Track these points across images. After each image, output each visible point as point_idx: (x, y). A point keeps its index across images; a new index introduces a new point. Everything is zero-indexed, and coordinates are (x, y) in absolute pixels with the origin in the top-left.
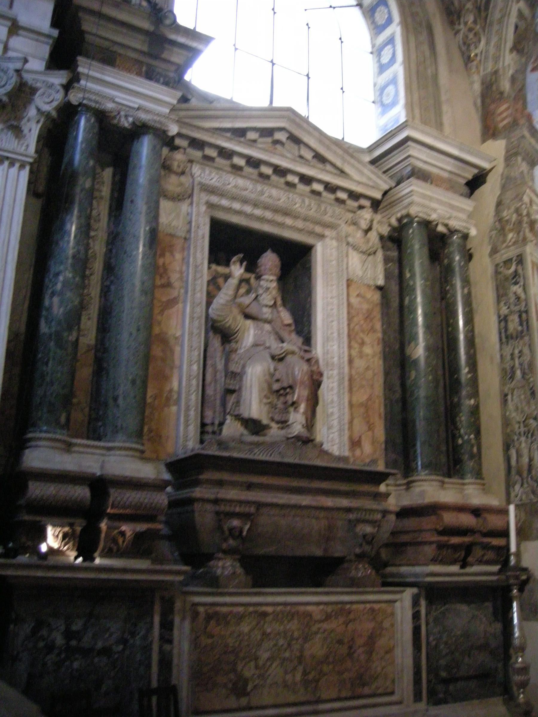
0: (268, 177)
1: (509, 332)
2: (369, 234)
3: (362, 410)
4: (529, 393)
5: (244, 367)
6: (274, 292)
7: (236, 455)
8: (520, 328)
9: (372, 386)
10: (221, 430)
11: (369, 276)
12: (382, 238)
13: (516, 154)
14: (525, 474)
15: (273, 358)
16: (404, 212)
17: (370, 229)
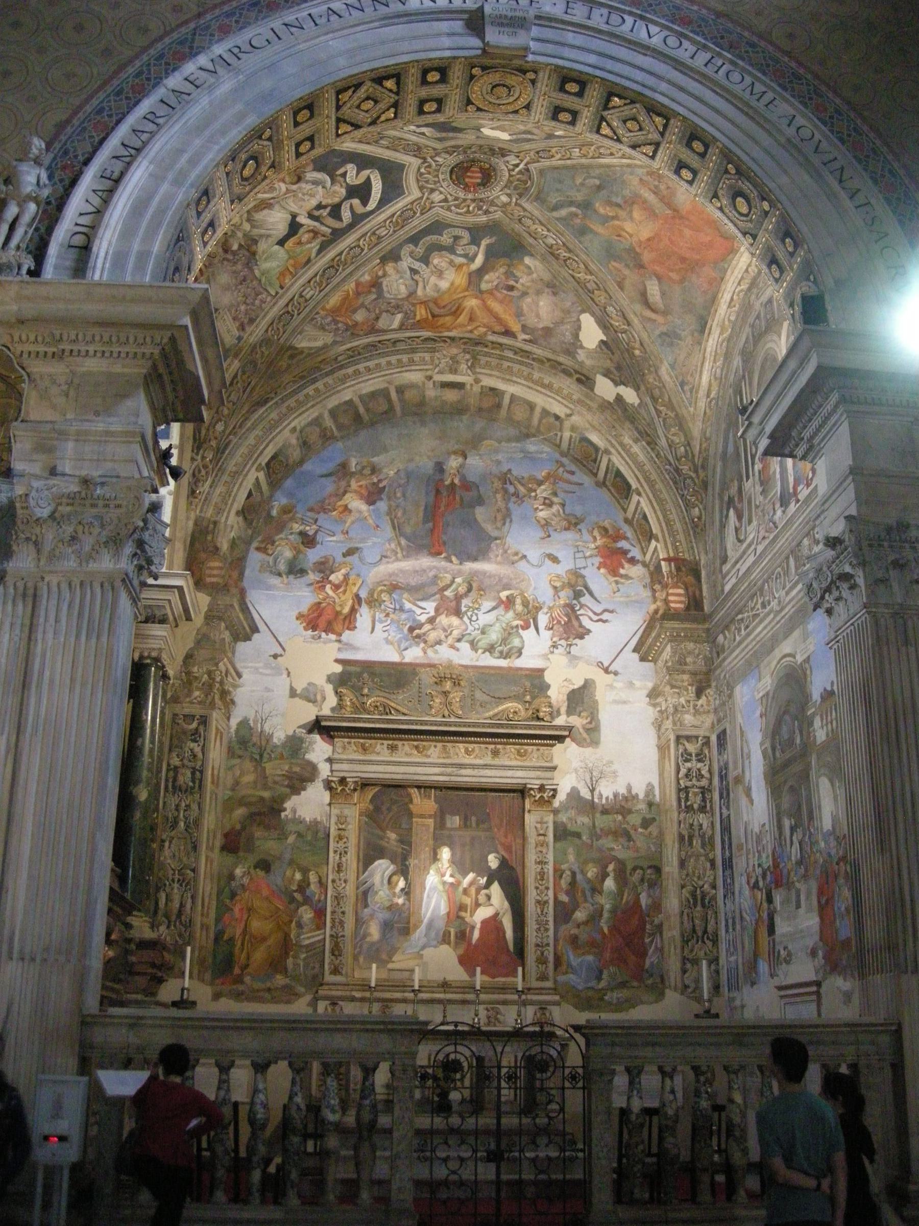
1: (178, 783)
4: (190, 846)
8: (191, 784)
13: (220, 619)
14: (173, 918)
16: (154, 654)
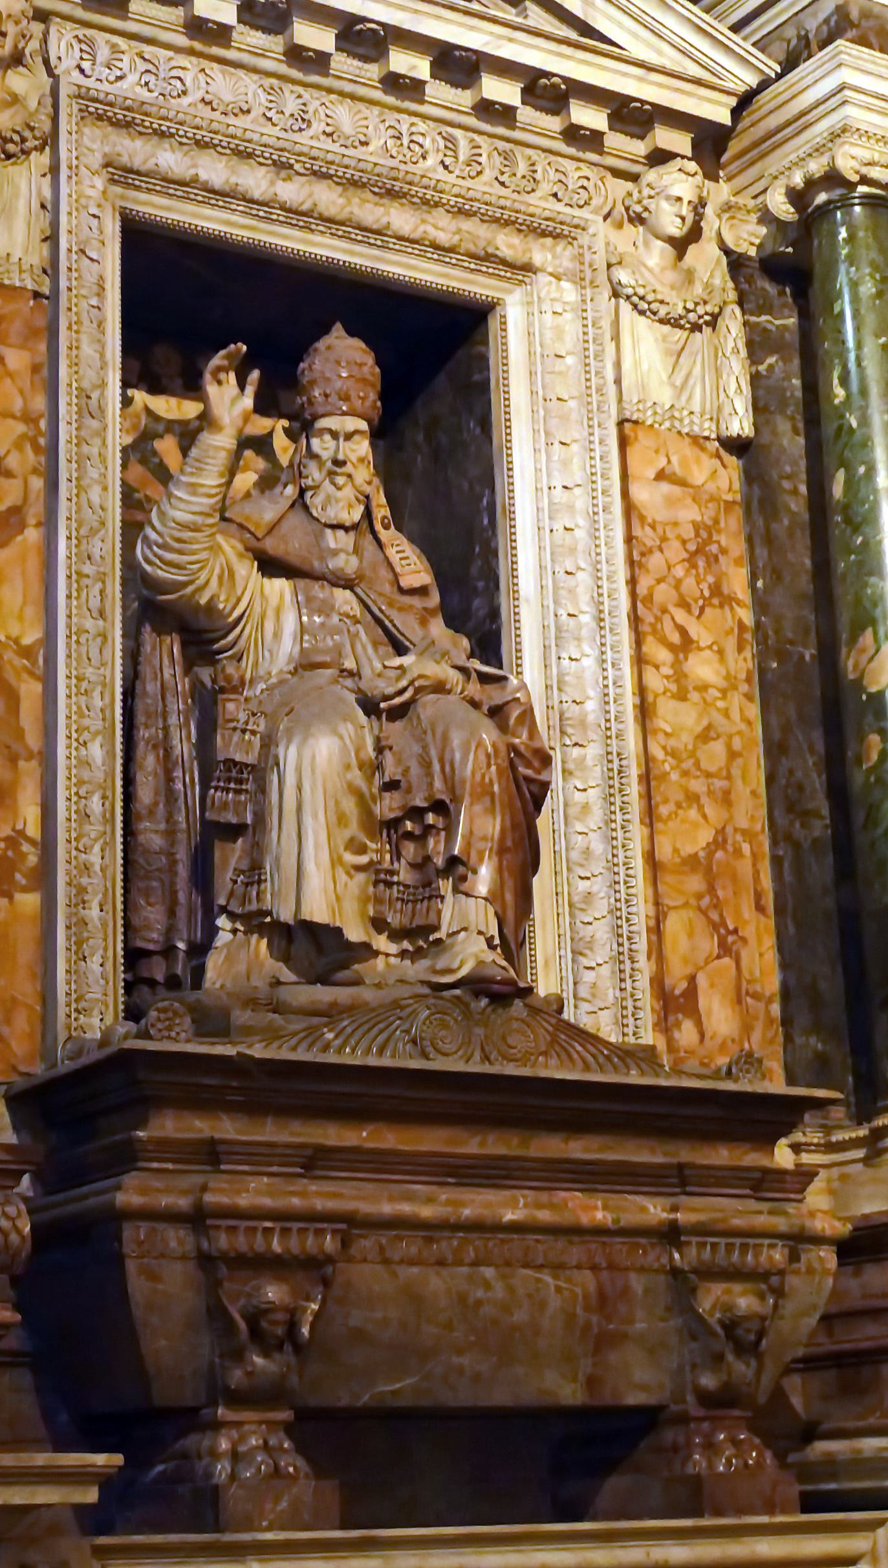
0: (320, 61)
2: (692, 249)
3: (695, 883)
5: (268, 742)
6: (363, 475)
7: (258, 1051)
9: (726, 799)
10: (199, 973)
11: (696, 406)
12: (736, 263)
15: (370, 706)
16: (816, 167)
17: (694, 234)
